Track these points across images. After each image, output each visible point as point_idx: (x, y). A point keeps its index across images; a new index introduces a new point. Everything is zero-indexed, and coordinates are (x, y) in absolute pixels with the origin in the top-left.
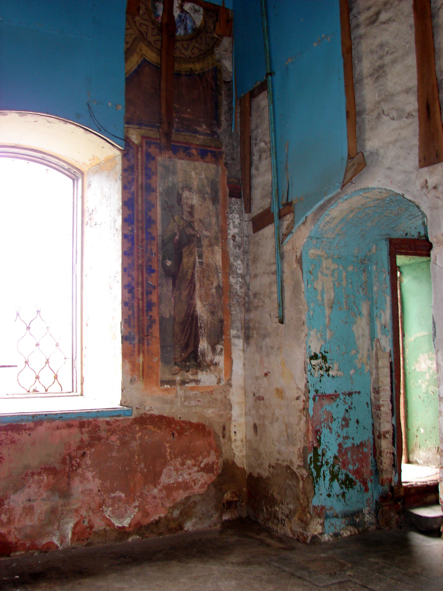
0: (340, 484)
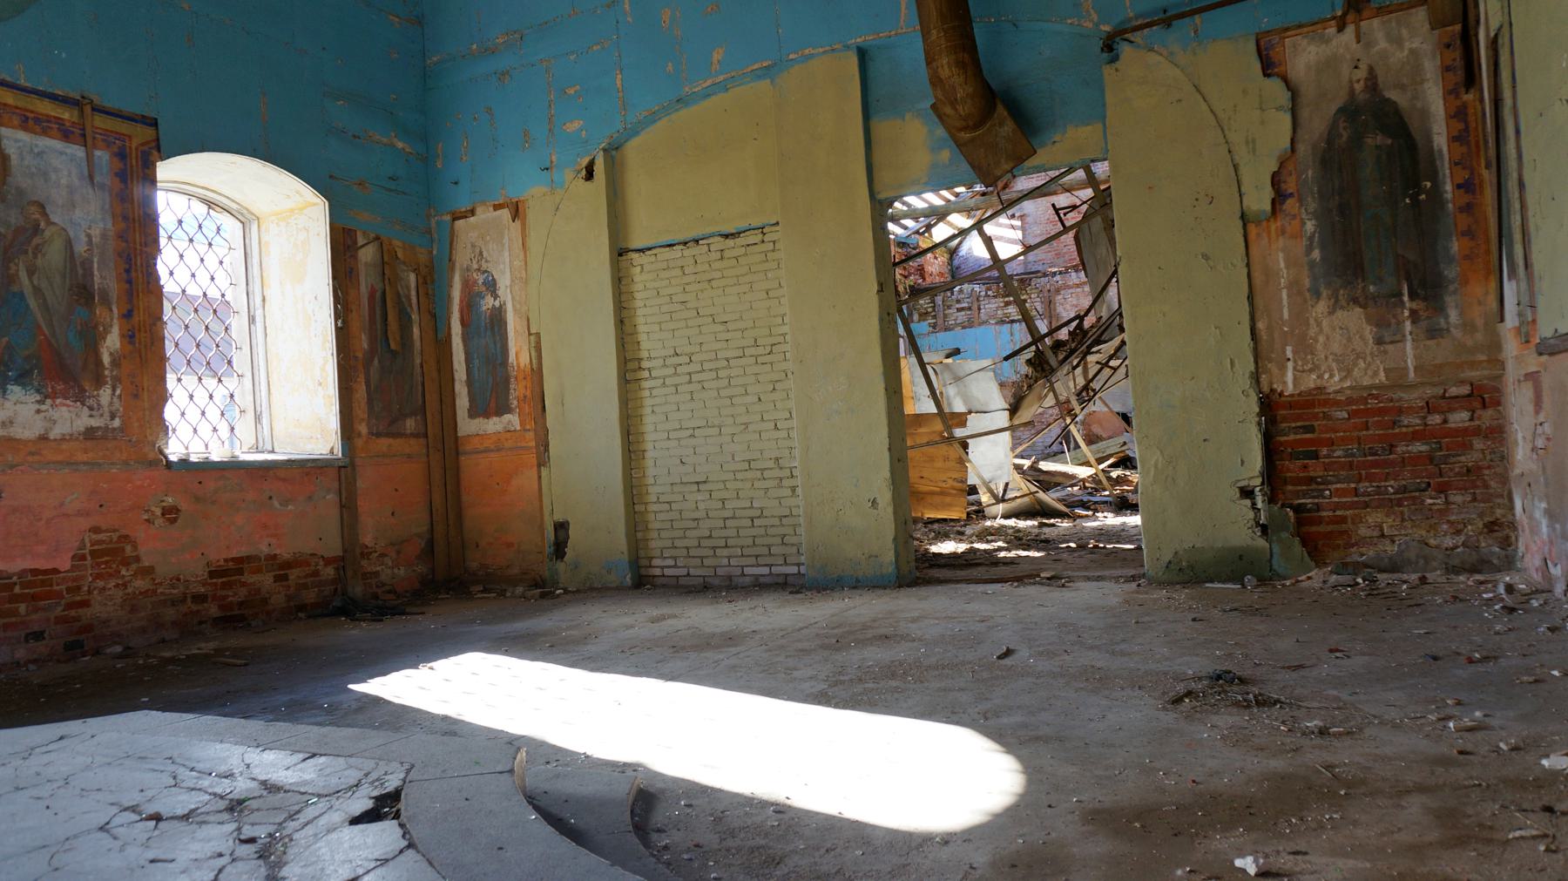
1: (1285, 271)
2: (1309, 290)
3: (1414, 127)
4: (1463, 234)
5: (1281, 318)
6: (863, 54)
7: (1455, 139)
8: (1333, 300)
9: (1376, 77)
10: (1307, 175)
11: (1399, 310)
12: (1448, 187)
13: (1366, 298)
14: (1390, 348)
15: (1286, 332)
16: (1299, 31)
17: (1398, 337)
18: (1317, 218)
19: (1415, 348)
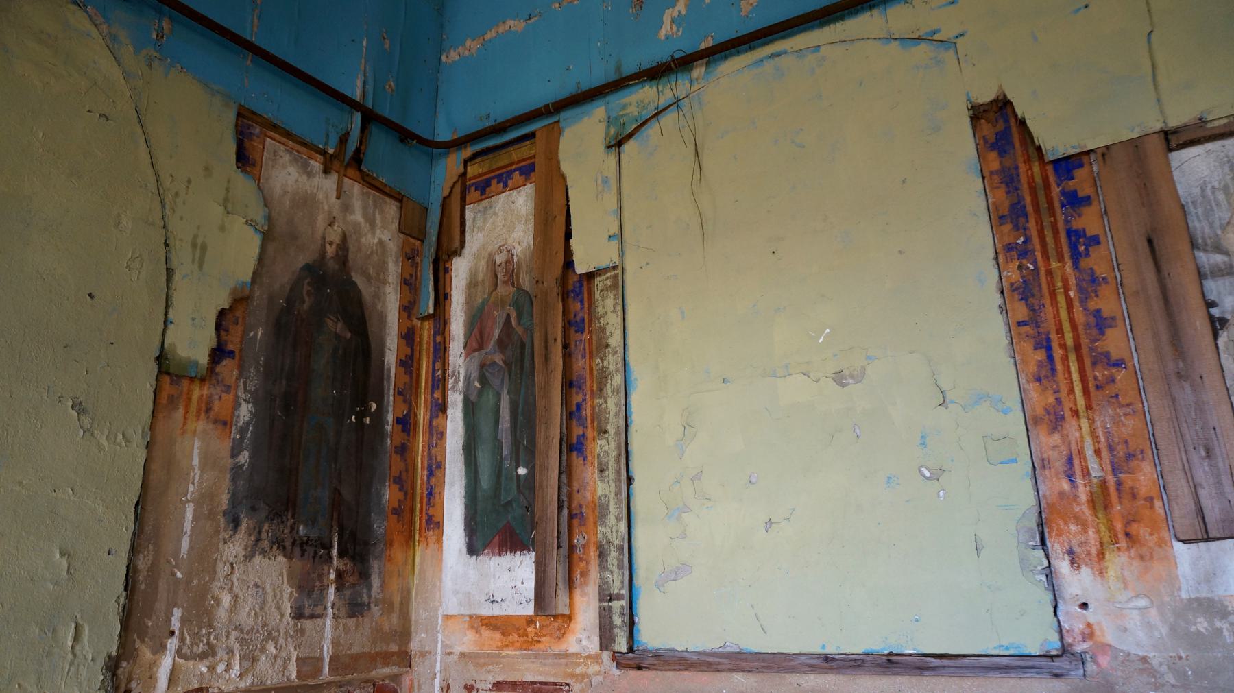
1: (198, 473)
2: (225, 513)
3: (372, 329)
4: (395, 482)
5: (176, 554)
7: (401, 363)
8: (253, 538)
9: (347, 250)
10: (256, 335)
11: (326, 568)
12: (390, 418)
13: (293, 544)
14: (308, 624)
15: (178, 581)
16: (283, 140)
17: (319, 610)
18: (255, 404)
19: (336, 628)
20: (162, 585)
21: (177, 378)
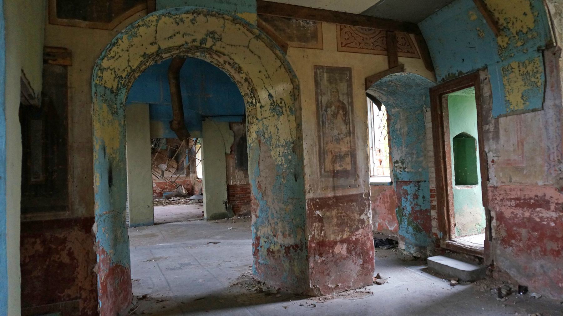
0: (413, 229)
6: (150, 105)
20: (230, 175)
21: (228, 155)
